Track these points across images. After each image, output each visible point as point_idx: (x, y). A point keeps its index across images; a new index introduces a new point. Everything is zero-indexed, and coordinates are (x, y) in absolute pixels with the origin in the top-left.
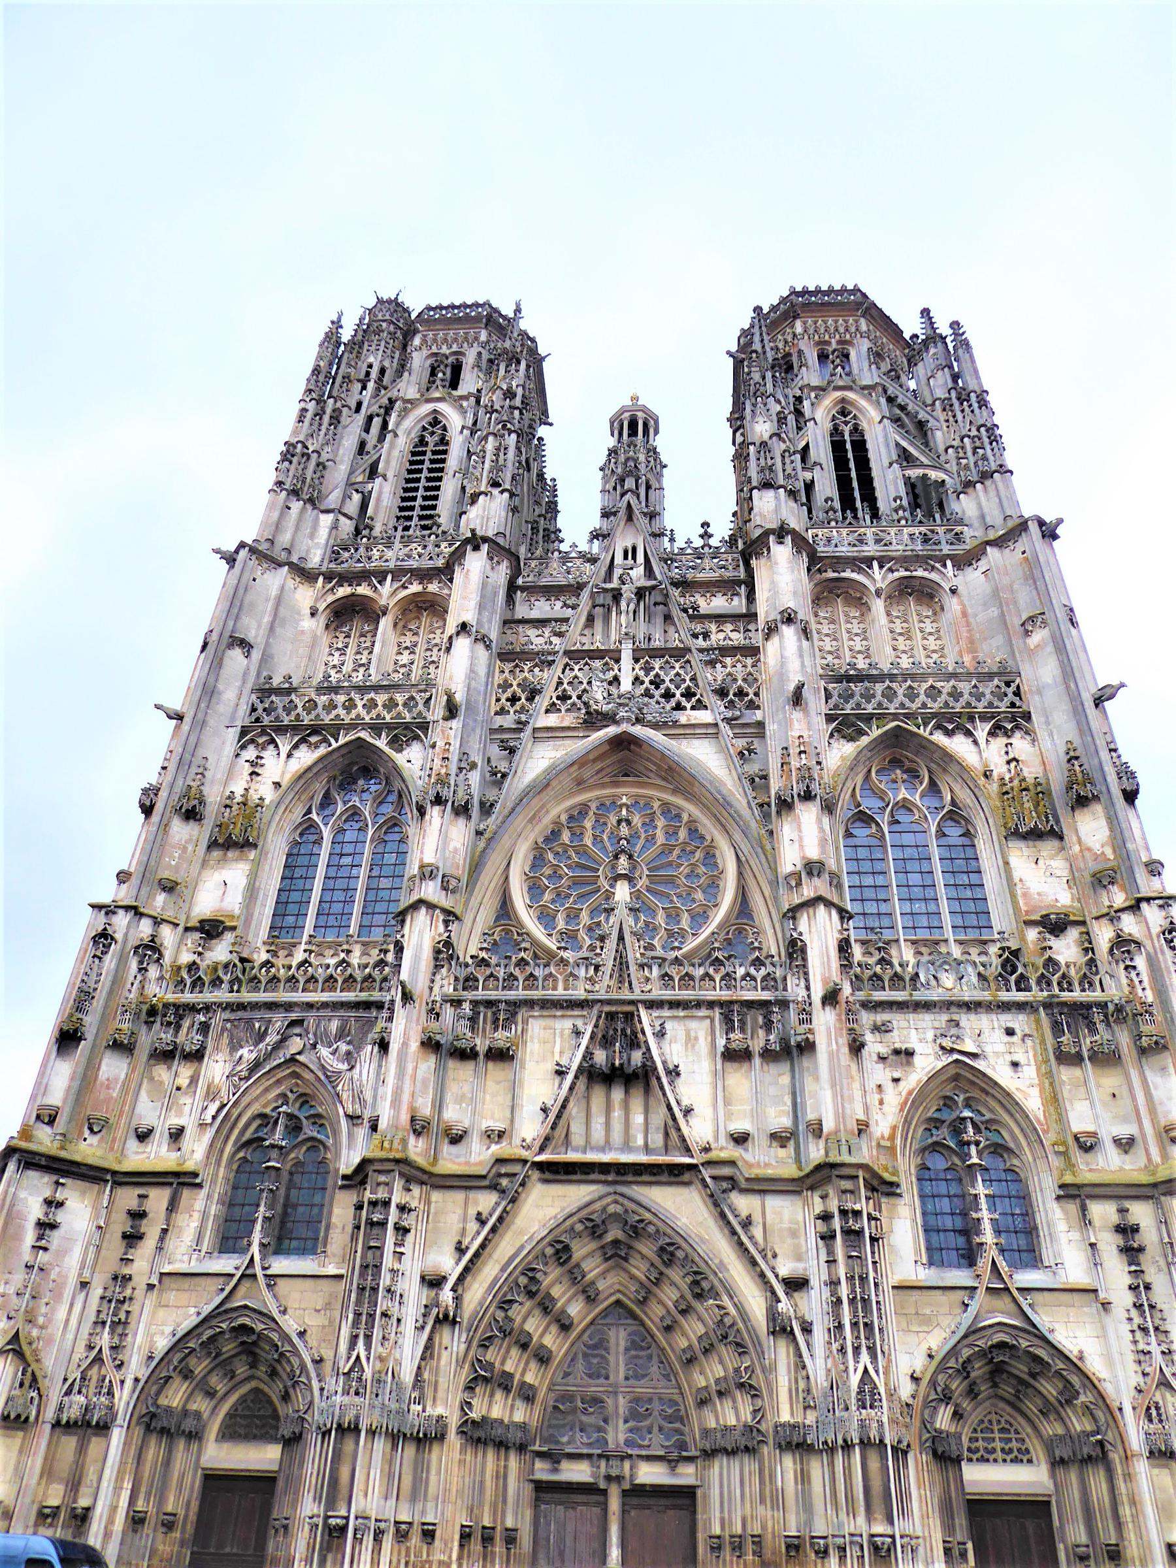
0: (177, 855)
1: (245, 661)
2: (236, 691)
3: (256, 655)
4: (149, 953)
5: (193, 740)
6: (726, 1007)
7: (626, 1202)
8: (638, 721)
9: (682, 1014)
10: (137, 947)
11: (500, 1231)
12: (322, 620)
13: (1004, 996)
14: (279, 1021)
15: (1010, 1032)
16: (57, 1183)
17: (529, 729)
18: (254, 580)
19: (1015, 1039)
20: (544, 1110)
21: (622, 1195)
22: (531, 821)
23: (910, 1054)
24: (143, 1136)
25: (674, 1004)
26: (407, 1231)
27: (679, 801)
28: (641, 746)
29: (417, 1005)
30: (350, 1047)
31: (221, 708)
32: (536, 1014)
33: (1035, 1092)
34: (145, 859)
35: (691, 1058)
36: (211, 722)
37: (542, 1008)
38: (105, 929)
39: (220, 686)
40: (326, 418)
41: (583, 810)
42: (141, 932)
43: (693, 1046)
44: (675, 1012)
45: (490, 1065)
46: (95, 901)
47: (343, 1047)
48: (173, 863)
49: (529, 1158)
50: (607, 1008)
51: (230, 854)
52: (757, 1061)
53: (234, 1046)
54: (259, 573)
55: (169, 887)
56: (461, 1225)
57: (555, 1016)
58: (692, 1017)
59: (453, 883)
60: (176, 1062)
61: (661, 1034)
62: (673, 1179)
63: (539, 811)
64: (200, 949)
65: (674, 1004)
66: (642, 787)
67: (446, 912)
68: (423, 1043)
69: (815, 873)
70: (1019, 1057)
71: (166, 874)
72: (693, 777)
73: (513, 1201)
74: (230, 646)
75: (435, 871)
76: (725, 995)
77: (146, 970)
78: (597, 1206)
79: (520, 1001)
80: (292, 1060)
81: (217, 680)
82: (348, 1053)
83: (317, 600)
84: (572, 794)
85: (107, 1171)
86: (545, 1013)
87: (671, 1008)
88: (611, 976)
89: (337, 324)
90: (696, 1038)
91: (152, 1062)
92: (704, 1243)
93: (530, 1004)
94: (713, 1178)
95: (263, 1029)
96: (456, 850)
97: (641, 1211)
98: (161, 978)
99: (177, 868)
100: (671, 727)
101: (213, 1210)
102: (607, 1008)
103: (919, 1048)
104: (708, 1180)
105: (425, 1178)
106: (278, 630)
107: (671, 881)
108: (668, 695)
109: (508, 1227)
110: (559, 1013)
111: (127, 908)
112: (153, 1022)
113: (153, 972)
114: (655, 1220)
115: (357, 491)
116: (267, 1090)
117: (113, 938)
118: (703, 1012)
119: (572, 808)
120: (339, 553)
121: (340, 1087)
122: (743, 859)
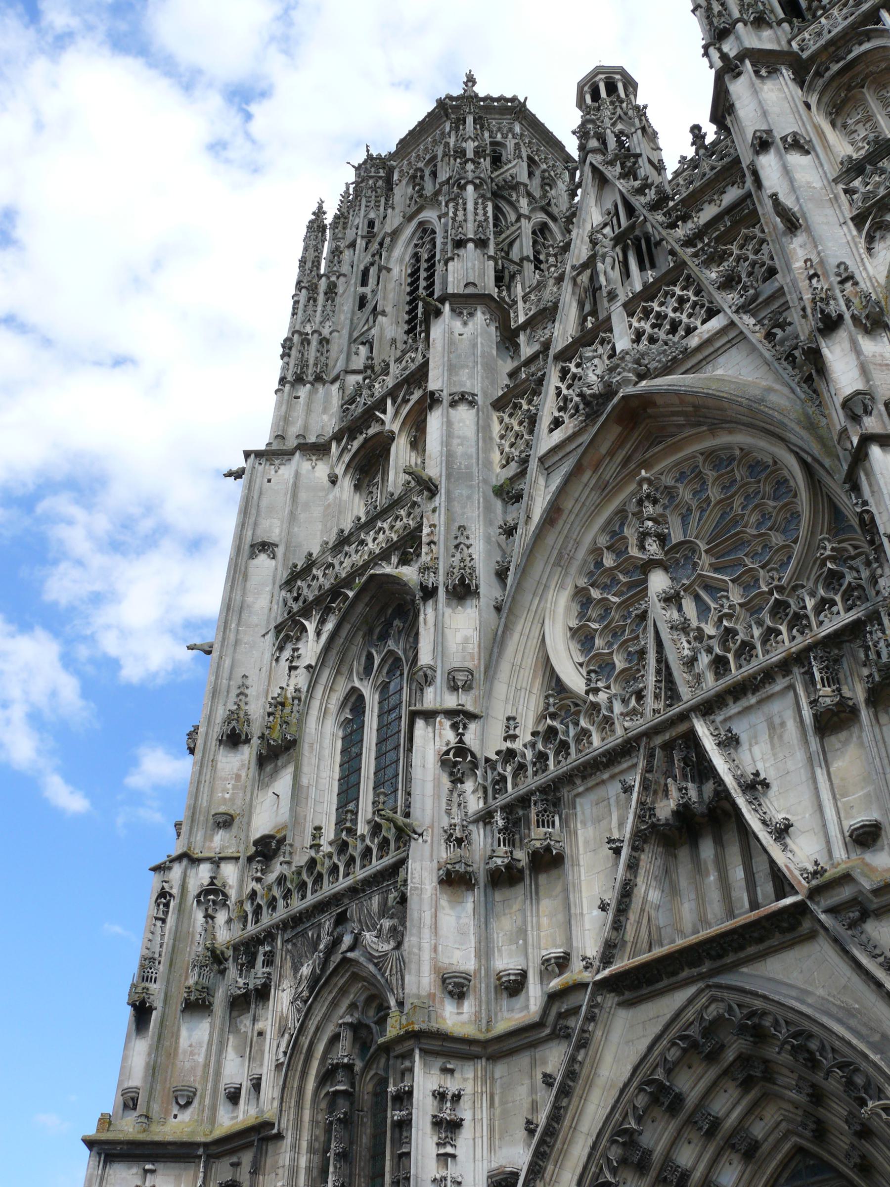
0: (230, 786)
1: (273, 562)
2: (269, 597)
3: (280, 551)
4: (212, 897)
5: (227, 663)
6: (800, 658)
7: (726, 995)
8: (641, 377)
9: (753, 700)
10: (199, 896)
11: (578, 1091)
12: (346, 484)
14: (327, 922)
16: (146, 1171)
17: (533, 464)
18: (269, 481)
20: (603, 907)
21: (719, 986)
22: (557, 564)
24: (234, 1097)
25: (738, 691)
26: (455, 1126)
27: (723, 439)
28: (654, 404)
29: (427, 837)
30: (395, 921)
31: (255, 620)
32: (581, 789)
34: (192, 802)
35: (781, 756)
36: (245, 638)
37: (584, 778)
38: (163, 888)
39: (249, 599)
40: (321, 298)
41: (621, 514)
42: (202, 878)
43: (781, 737)
44: (744, 703)
45: (543, 879)
46: (153, 865)
47: (387, 923)
48: (227, 796)
49: (588, 980)
50: (658, 740)
51: (280, 763)
52: (865, 714)
53: (296, 969)
54: (273, 472)
55: (225, 822)
56: (530, 1099)
57: (603, 782)
58: (770, 697)
59: (461, 677)
60: (253, 1006)
61: (729, 743)
62: (789, 936)
63: (564, 546)
64: (259, 874)
65: (738, 691)
66: (680, 449)
67: (450, 713)
68: (441, 882)
69: (859, 411)
71: (222, 809)
72: (719, 398)
73: (583, 1044)
74: (252, 556)
75: (429, 672)
76: (801, 641)
77: (213, 918)
78: (690, 1014)
79: (553, 781)
80: (345, 960)
81: (244, 595)
82: (393, 929)
83: (332, 468)
84: (598, 508)
85: (197, 1145)
86: (591, 783)
87: (736, 699)
88: (657, 697)
89: (319, 213)
90: (783, 724)
91: (235, 1014)
92: (853, 1016)
93: (567, 779)
94: (828, 911)
95: (315, 936)
96: (466, 640)
97: (748, 1000)
98: (229, 921)
99: (232, 799)
100: (683, 361)
101: (303, 1162)
102: (658, 740)
104: (823, 917)
105: (475, 1049)
106: (302, 516)
107: (740, 542)
108: (674, 327)
109: (590, 1083)
110: (606, 776)
111: (179, 858)
112: (225, 969)
113: (221, 917)
114: (769, 1007)
115: (363, 343)
116: (334, 1004)
117: (171, 895)
118: (780, 684)
119: (609, 522)
120: (348, 409)
121: (388, 973)
122: (809, 460)
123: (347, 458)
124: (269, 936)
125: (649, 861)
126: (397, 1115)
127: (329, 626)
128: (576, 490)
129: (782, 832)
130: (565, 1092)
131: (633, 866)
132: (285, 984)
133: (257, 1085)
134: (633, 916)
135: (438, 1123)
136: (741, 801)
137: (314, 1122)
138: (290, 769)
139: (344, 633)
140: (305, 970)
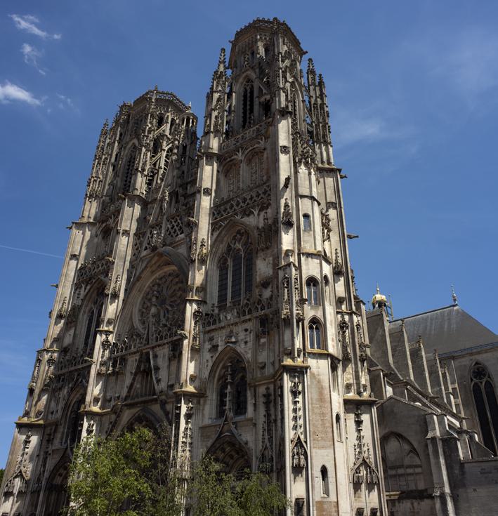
8: (164, 245)
12: (100, 237)
13: (243, 318)
14: (76, 374)
15: (246, 330)
19: (248, 333)
22: (139, 291)
23: (218, 346)
33: (250, 352)
53: (69, 384)
61: (156, 356)
65: (159, 346)
67: (106, 331)
70: (248, 339)
74: (71, 259)
103: (220, 344)
123: (101, 229)
124: (64, 374)
125: (139, 378)
126: (80, 428)
127: (88, 287)
128: (145, 272)
129: (159, 381)
130: (114, 426)
131: (134, 379)
132: (66, 387)
133: (57, 411)
134: (133, 390)
135: (87, 431)
136: (153, 372)
137: (69, 422)
138: (74, 328)
139: (92, 290)
140: (70, 385)
